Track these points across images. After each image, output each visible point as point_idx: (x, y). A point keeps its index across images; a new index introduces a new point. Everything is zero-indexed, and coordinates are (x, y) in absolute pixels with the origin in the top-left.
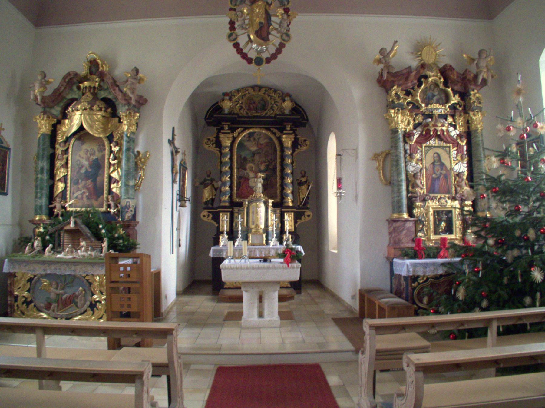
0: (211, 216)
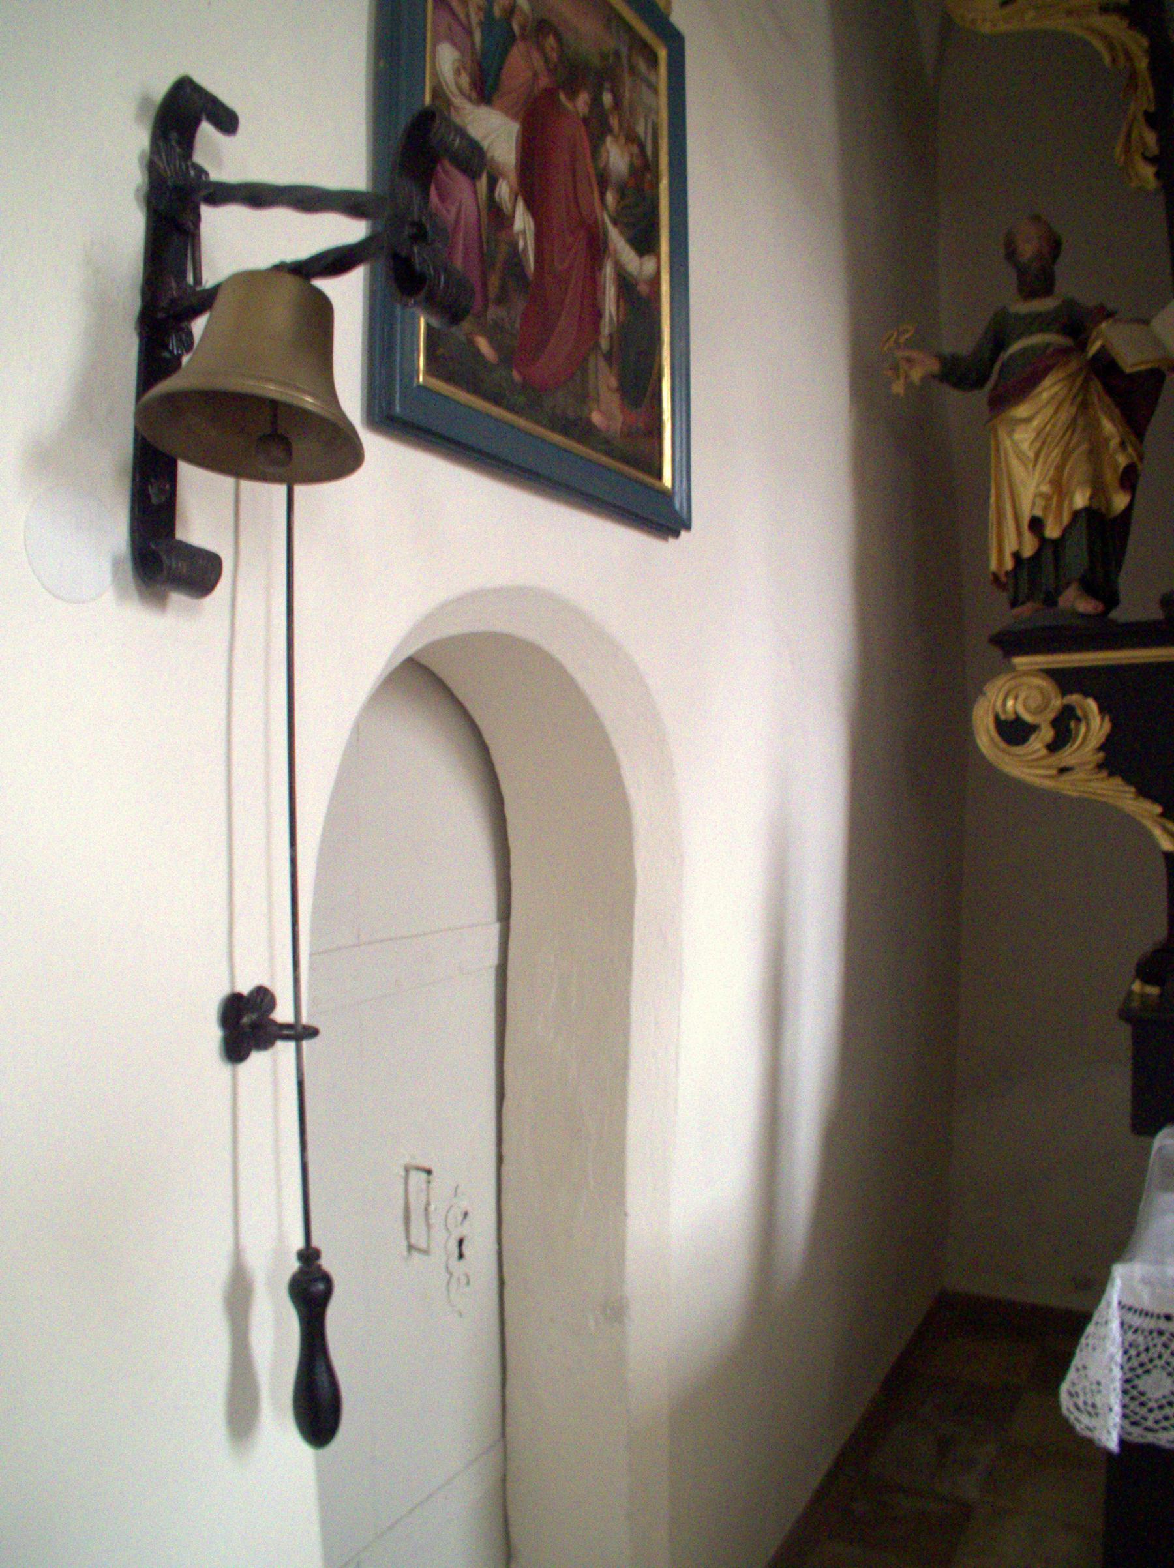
0: (1095, 726)
